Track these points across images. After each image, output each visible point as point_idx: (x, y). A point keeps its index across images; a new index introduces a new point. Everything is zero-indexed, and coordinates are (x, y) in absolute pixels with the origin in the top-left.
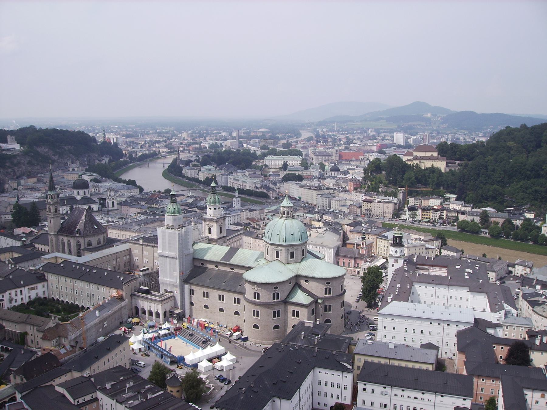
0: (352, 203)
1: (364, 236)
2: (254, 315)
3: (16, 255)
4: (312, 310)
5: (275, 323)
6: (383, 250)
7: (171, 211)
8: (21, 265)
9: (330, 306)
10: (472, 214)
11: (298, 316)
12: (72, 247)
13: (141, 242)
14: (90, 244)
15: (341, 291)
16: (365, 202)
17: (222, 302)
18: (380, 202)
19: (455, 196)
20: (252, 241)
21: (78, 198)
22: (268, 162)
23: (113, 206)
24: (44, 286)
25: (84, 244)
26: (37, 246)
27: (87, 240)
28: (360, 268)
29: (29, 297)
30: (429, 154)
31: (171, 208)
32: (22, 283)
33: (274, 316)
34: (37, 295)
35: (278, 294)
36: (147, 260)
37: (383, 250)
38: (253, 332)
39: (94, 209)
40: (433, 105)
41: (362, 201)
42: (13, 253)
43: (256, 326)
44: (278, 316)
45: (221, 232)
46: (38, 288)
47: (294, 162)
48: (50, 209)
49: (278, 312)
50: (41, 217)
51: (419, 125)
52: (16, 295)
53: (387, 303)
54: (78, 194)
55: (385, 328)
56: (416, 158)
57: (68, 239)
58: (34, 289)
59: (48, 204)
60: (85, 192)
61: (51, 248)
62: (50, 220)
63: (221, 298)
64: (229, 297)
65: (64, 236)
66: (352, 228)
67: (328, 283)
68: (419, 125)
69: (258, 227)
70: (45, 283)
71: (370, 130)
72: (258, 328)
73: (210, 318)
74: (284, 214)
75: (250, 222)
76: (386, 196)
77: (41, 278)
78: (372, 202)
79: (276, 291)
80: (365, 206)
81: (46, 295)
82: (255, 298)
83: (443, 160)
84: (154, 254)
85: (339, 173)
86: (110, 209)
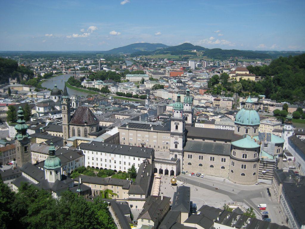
0: (206, 101)
2: (242, 168)
7: (179, 107)
10: (278, 106)
12: (81, 133)
13: (127, 127)
19: (265, 96)
21: (55, 101)
25: (89, 130)
26: (49, 133)
30: (244, 73)
33: (254, 168)
34: (79, 165)
36: (131, 139)
38: (241, 178)
40: (195, 44)
42: (37, 139)
43: (243, 174)
44: (256, 167)
48: (64, 108)
49: (256, 164)
51: (191, 56)
52: (69, 166)
56: (237, 75)
57: (78, 127)
59: (63, 105)
61: (64, 134)
62: (65, 115)
63: (212, 159)
64: (218, 158)
65: (75, 125)
67: (279, 146)
68: (191, 56)
70: (83, 156)
71: (165, 60)
74: (249, 107)
76: (226, 97)
78: (220, 100)
80: (215, 103)
82: (243, 157)
83: (254, 76)
84: (138, 135)
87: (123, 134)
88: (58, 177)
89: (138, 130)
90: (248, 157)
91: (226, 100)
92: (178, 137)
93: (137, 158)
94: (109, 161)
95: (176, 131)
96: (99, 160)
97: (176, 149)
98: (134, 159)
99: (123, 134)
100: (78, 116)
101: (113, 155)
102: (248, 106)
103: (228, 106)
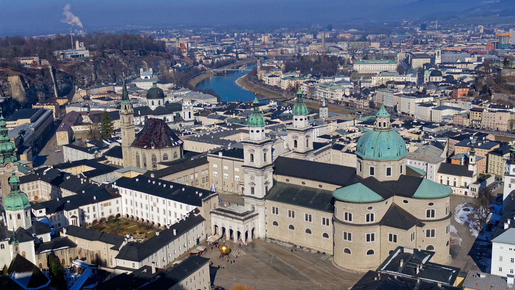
1: (473, 151)
2: (345, 238)
3: (87, 169)
4: (412, 234)
5: (368, 247)
6: (496, 168)
8: (94, 179)
9: (433, 231)
11: (395, 241)
13: (220, 154)
14: (165, 158)
15: (446, 214)
16: (472, 112)
17: (310, 222)
18: (492, 111)
20: (341, 155)
21: (153, 108)
22: (358, 67)
23: (190, 117)
24: (117, 202)
26: (109, 158)
27: (163, 151)
28: (468, 188)
29: (102, 214)
31: (253, 119)
32: (95, 198)
33: (368, 240)
34: (111, 212)
35: (372, 215)
37: (496, 168)
39: (169, 120)
41: (469, 111)
44: (373, 240)
45: (307, 146)
46: (112, 204)
47: (387, 67)
49: (373, 235)
50: (113, 128)
53: (503, 230)
54: (153, 104)
55: (501, 259)
58: (108, 205)
60: (159, 101)
63: (309, 218)
66: (458, 142)
67: (431, 204)
69: (348, 140)
70: (119, 199)
72: (350, 253)
73: (296, 240)
74: (380, 126)
75: (339, 134)
77: (115, 195)
79: (371, 212)
81: (120, 212)
82: (346, 219)
85: (441, 77)
86: (186, 120)
87: (215, 166)
88: (22, 222)
89: (235, 160)
90: (354, 218)
91: (497, 110)
92: (254, 173)
93: (184, 205)
94: (151, 208)
95: (252, 164)
96: (139, 205)
97: (252, 195)
98: (181, 208)
99: (215, 166)
100: (146, 134)
101: (155, 198)
102: (382, 125)
103: (499, 124)
